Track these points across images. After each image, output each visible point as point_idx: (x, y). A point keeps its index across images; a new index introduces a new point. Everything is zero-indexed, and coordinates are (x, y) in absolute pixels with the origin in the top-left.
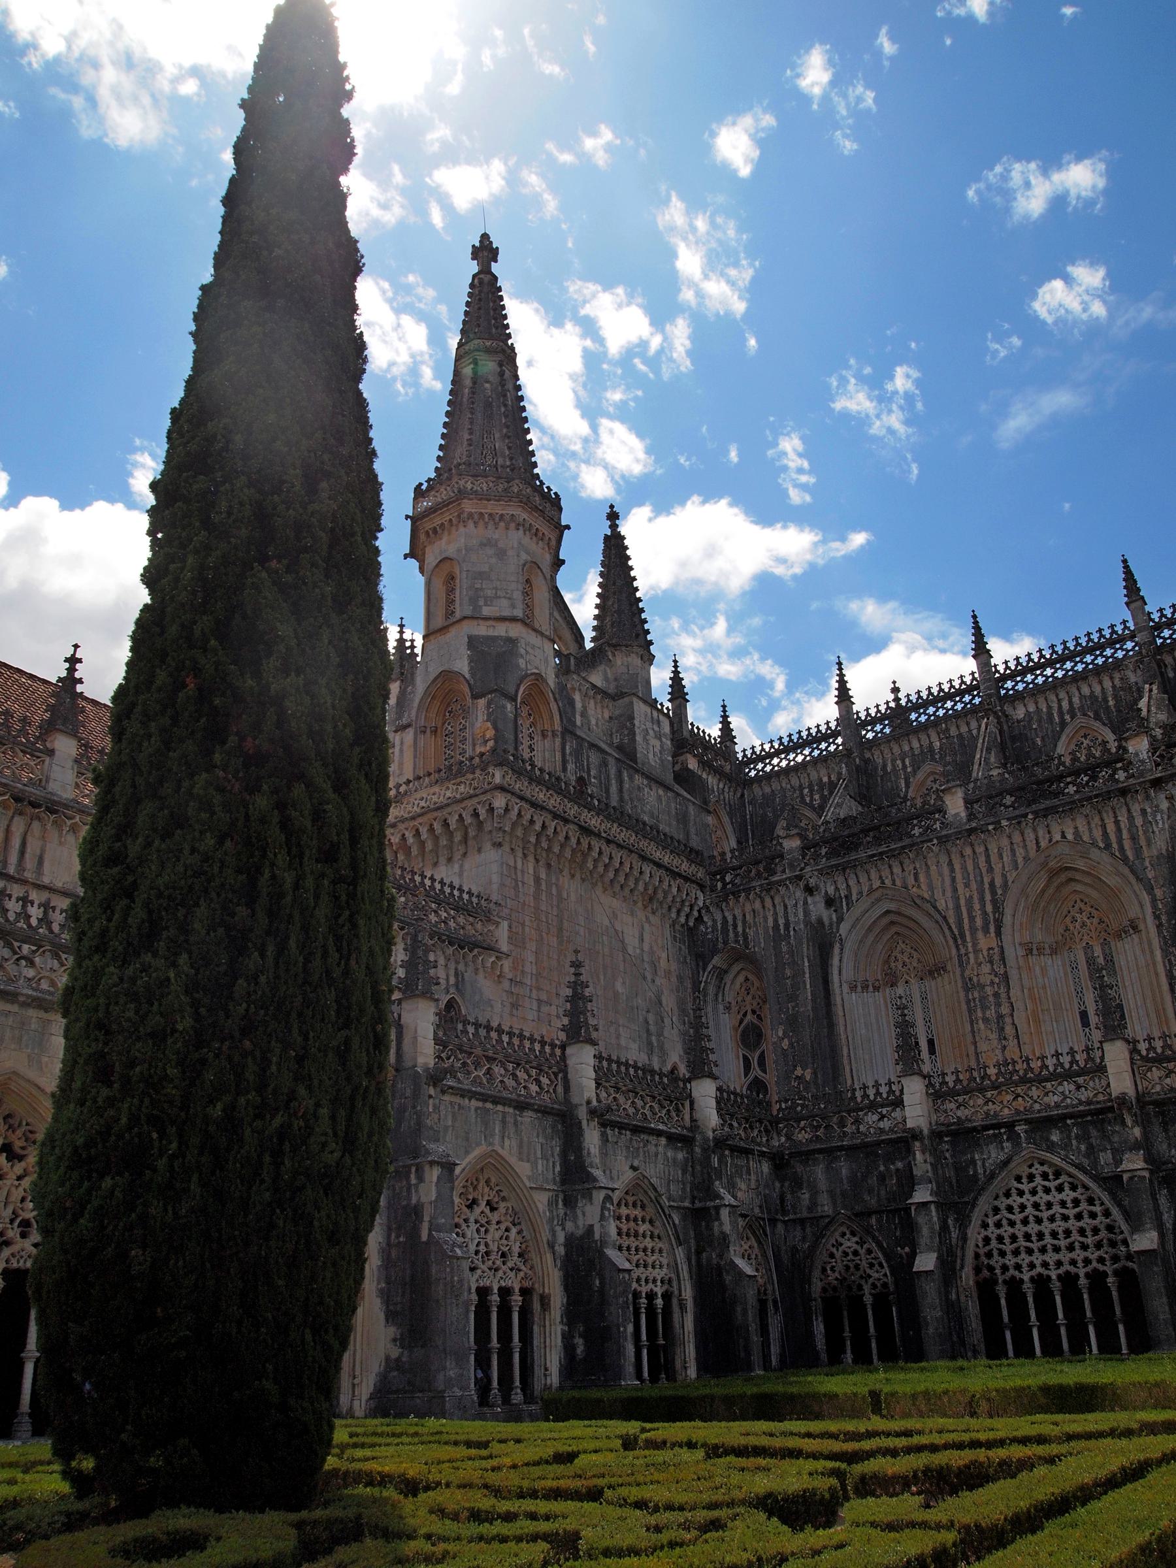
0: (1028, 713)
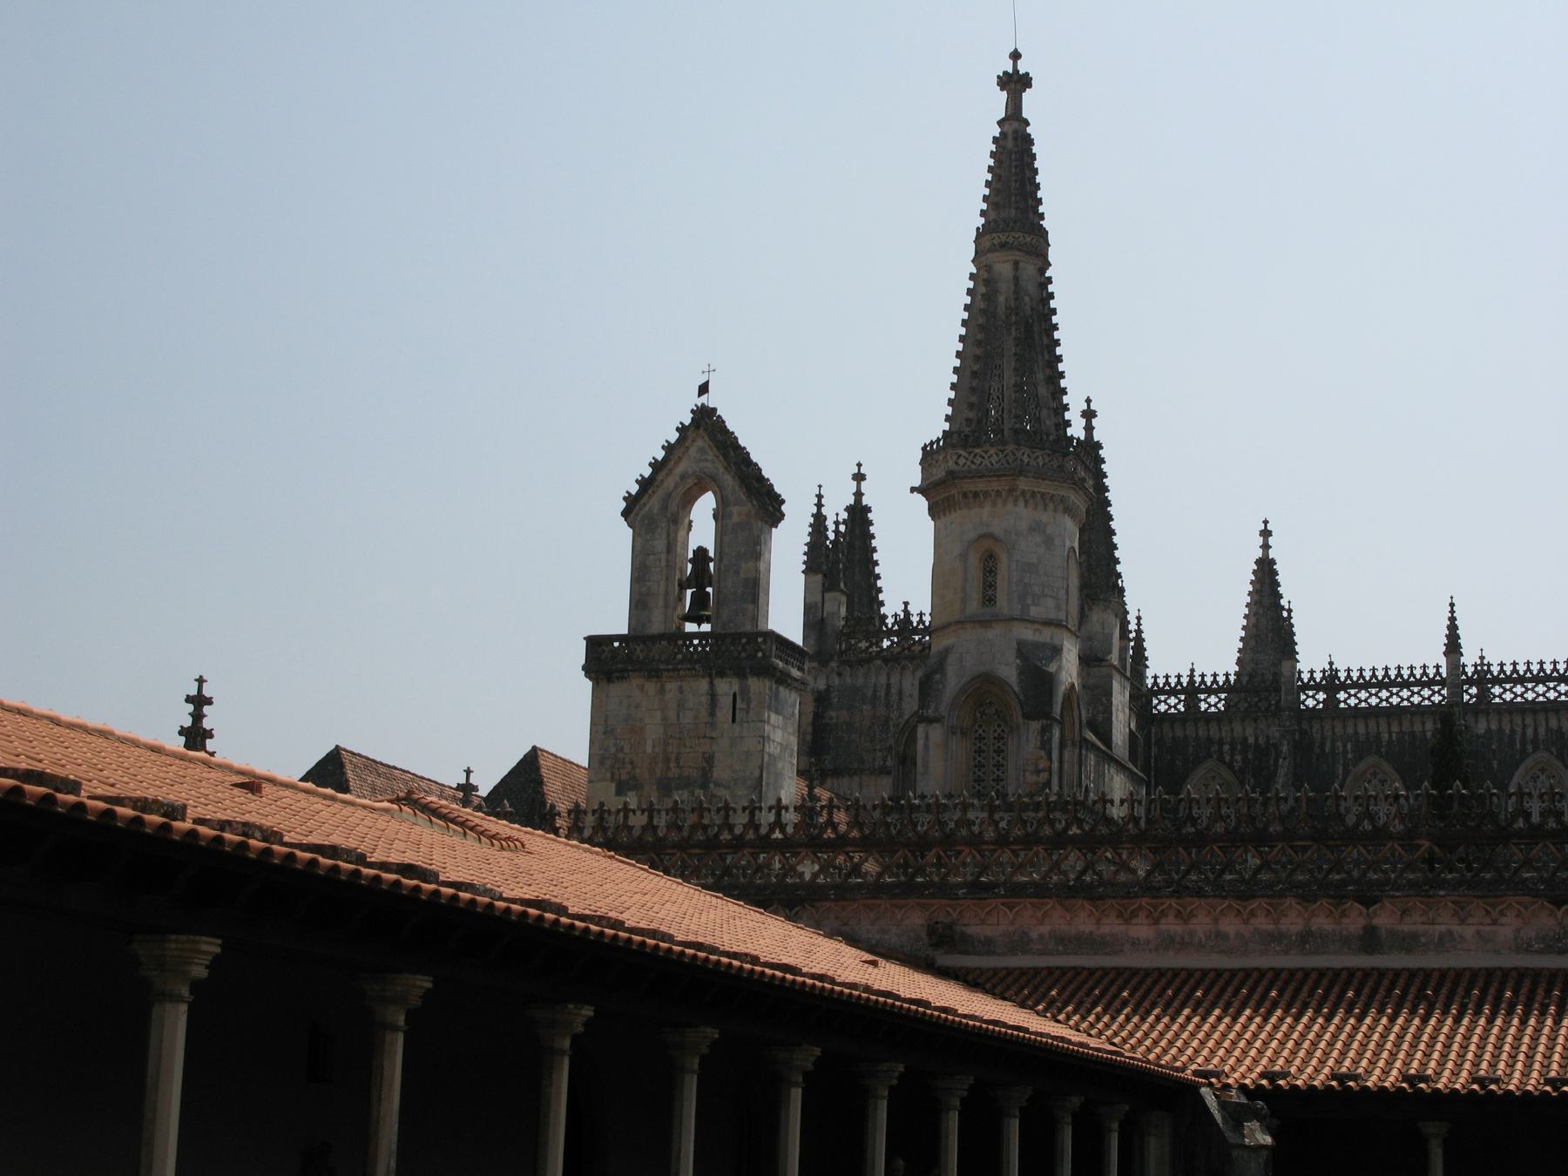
0: (1489, 730)
